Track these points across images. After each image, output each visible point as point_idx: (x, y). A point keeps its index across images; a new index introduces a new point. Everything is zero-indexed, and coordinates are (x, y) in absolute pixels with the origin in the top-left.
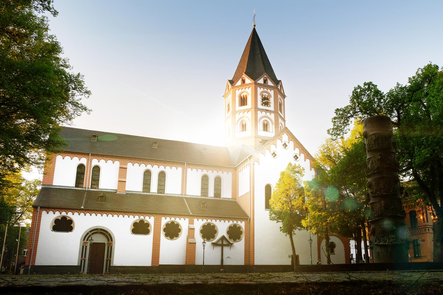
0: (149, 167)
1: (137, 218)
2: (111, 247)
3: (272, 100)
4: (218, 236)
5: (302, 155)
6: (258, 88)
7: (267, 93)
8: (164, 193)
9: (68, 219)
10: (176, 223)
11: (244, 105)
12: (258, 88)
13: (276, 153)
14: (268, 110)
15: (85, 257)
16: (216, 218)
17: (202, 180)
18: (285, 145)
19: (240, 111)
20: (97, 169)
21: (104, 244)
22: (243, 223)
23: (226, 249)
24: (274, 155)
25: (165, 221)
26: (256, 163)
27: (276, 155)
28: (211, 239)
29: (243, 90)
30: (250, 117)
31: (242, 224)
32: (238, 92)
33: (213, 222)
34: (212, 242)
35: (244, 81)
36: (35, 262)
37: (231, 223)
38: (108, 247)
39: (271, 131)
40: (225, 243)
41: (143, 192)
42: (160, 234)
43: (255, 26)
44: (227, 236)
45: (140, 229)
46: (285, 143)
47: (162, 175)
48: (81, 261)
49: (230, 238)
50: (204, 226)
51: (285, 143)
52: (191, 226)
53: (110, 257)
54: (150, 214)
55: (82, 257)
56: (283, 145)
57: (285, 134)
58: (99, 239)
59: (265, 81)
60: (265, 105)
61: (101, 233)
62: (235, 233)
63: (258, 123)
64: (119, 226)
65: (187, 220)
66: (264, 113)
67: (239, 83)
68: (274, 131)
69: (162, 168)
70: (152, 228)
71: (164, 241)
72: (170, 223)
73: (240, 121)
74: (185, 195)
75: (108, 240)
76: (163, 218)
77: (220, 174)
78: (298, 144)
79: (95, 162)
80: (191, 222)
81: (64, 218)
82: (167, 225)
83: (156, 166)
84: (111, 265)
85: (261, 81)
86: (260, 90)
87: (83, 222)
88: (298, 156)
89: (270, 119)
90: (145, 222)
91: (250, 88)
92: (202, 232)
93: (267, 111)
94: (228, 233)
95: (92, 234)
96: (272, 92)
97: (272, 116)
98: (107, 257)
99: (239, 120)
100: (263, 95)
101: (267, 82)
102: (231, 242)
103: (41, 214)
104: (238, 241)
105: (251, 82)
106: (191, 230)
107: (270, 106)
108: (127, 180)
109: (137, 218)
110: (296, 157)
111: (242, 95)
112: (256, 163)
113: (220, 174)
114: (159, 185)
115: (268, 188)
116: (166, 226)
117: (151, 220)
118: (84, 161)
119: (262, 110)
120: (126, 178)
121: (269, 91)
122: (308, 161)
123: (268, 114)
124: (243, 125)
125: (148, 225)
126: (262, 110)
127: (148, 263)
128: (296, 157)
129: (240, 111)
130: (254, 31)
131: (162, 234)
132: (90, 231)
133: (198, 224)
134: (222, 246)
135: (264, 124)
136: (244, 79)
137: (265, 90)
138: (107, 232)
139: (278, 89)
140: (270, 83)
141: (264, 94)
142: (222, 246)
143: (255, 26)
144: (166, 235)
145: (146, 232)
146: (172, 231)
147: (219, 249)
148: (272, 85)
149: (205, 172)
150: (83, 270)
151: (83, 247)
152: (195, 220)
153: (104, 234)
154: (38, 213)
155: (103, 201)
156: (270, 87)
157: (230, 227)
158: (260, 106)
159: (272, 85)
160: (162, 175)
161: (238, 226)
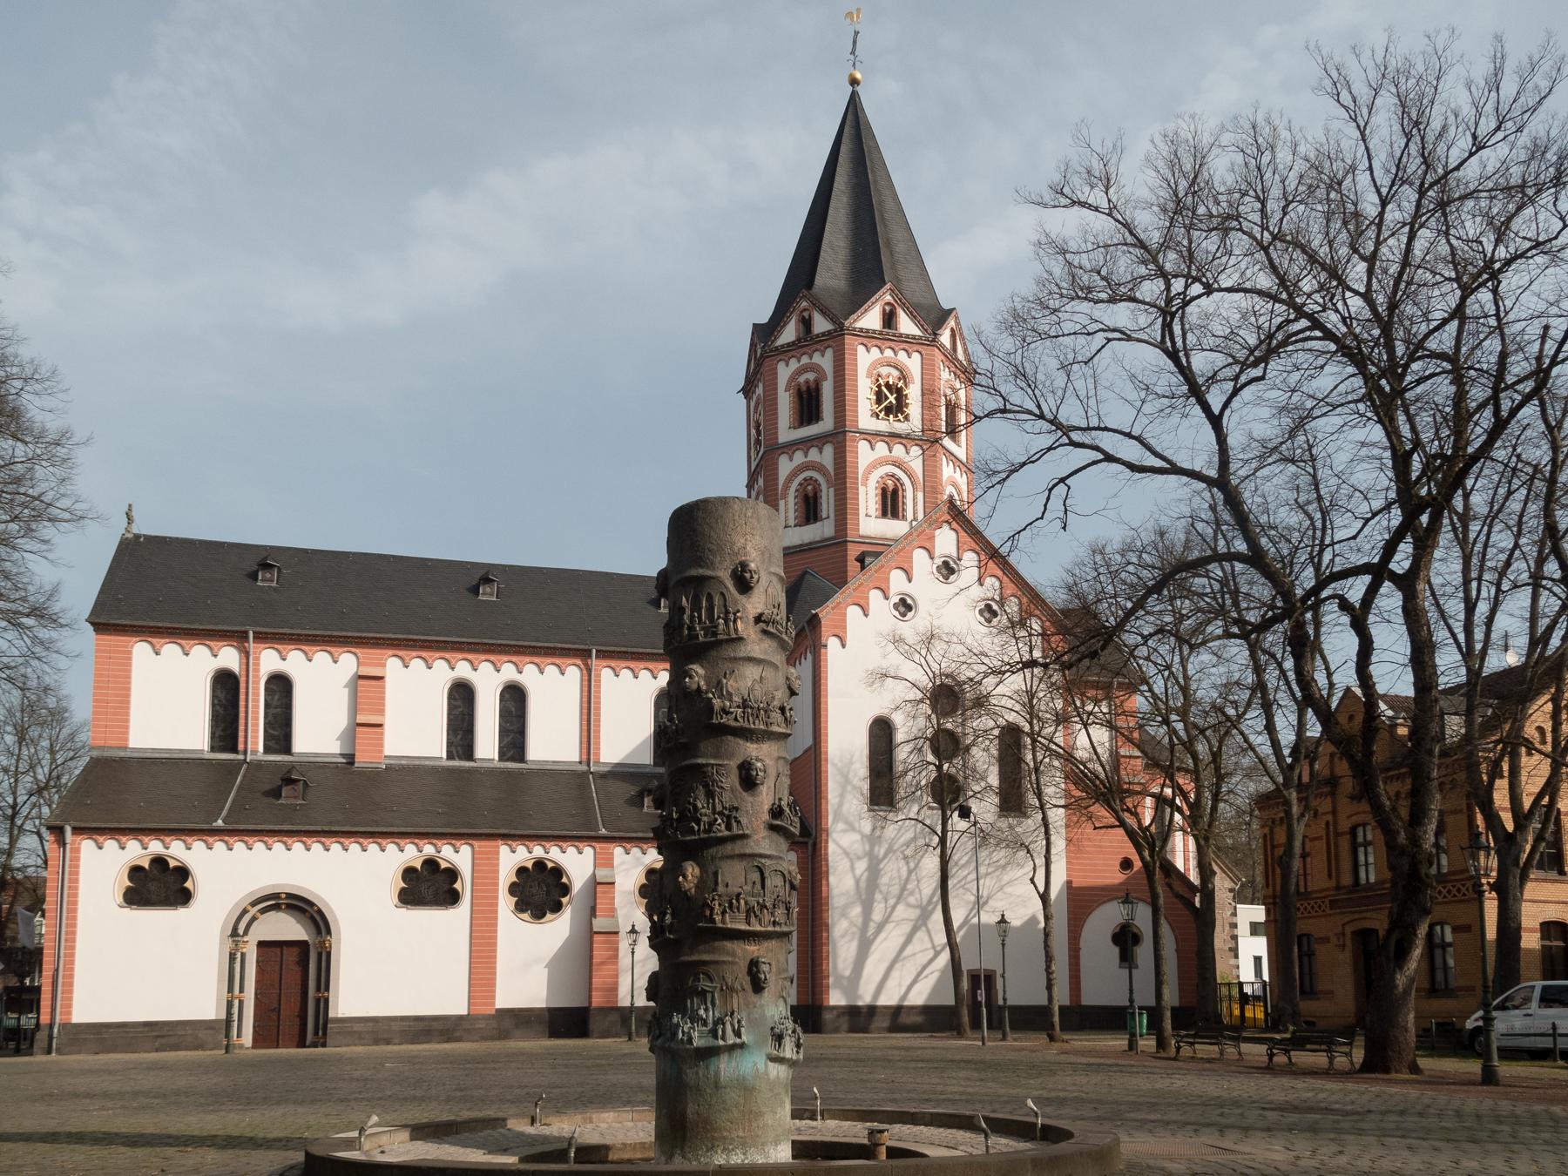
0: (463, 670)
1: (412, 854)
2: (329, 954)
3: (913, 393)
10: (550, 865)
14: (898, 436)
15: (241, 990)
19: (791, 447)
21: (305, 942)
27: (909, 608)
29: (805, 360)
32: (784, 372)
36: (69, 1013)
38: (320, 955)
42: (496, 905)
45: (428, 887)
48: (230, 1005)
52: (602, 874)
53: (327, 989)
55: (230, 989)
58: (288, 928)
59: (889, 319)
60: (887, 415)
61: (289, 907)
64: (353, 880)
65: (588, 851)
66: (881, 448)
67: (789, 334)
69: (509, 672)
70: (465, 885)
71: (510, 924)
72: (529, 865)
75: (319, 932)
76: (504, 850)
79: (269, 660)
80: (604, 861)
82: (522, 871)
84: (331, 1014)
87: (228, 872)
90: (444, 865)
91: (829, 353)
92: (644, 891)
96: (913, 364)
98: (318, 990)
99: (789, 480)
109: (412, 854)
111: (802, 379)
117: (459, 856)
118: (229, 657)
119: (872, 437)
120: (382, 712)
123: (899, 450)
125: (453, 874)
126: (872, 437)
127: (455, 1003)
129: (791, 447)
131: (506, 903)
132: (253, 904)
138: (311, 904)
139: (941, 347)
141: (885, 371)
144: (520, 907)
145: (453, 898)
148: (916, 331)
152: (618, 851)
153: (303, 911)
159: (916, 331)
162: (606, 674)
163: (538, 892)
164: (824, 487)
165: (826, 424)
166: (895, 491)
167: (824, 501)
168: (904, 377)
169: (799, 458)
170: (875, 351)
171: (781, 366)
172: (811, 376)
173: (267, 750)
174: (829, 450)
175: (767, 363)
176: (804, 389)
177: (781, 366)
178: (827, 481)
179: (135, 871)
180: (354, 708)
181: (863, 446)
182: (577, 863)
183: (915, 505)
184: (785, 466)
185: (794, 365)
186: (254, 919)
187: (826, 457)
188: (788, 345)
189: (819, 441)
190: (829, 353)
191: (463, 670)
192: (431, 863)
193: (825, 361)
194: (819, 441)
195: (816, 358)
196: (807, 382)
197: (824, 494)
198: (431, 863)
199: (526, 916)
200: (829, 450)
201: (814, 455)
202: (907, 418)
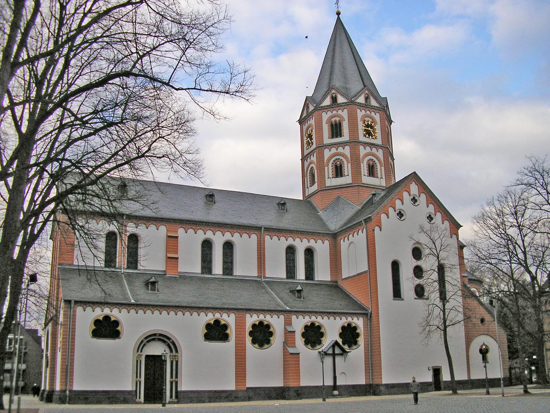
0: (209, 235)
2: (177, 362)
3: (378, 128)
4: (327, 342)
5: (439, 215)
6: (358, 110)
8: (231, 274)
9: (113, 319)
11: (337, 137)
13: (402, 212)
15: (140, 378)
16: (322, 313)
17: (287, 254)
18: (414, 200)
20: (134, 239)
22: (361, 319)
23: (338, 359)
24: (400, 215)
25: (251, 320)
26: (377, 229)
28: (318, 347)
29: (335, 112)
30: (348, 155)
31: (359, 322)
32: (325, 116)
33: (319, 320)
34: (320, 350)
35: (334, 99)
37: (343, 321)
39: (379, 176)
40: (337, 351)
41: (202, 273)
43: (338, 14)
44: (340, 341)
45: (216, 332)
46: (414, 198)
47: (228, 246)
49: (344, 344)
50: (306, 327)
51: (414, 198)
54: (229, 310)
56: (412, 199)
57: (414, 183)
58: (156, 349)
61: (159, 340)
62: (349, 335)
65: (282, 317)
66: (368, 149)
68: (384, 177)
69: (228, 236)
70: (232, 331)
71: (251, 349)
73: (331, 161)
74: (265, 277)
76: (248, 316)
77: (312, 243)
78: (432, 198)
79: (131, 228)
81: (107, 318)
82: (254, 326)
83: (219, 234)
84: (179, 389)
86: (360, 114)
88: (432, 216)
89: (377, 158)
91: (346, 110)
93: (372, 145)
94: (341, 335)
95: (148, 342)
96: (377, 117)
97: (380, 153)
98: (172, 377)
100: (365, 121)
101: (370, 101)
102: (347, 350)
103: (75, 311)
104: (355, 347)
105: (346, 101)
106: (289, 334)
107: (376, 138)
108: (180, 255)
110: (430, 218)
111: (333, 120)
112: (377, 229)
113: (312, 243)
114: (224, 262)
115: (395, 266)
116: (252, 327)
117: (229, 319)
119: (365, 144)
120: (177, 252)
121: (373, 114)
122: (446, 223)
123: (374, 150)
124: (336, 167)
126: (365, 144)
128: (430, 218)
131: (249, 340)
132: (146, 338)
133: (299, 324)
134: (334, 355)
135: (369, 165)
136: (334, 95)
137: (368, 112)
138: (169, 339)
140: (373, 103)
141: (367, 119)
142: (334, 355)
143: (338, 14)
144: (254, 342)
145: (225, 337)
146: (262, 335)
147: (328, 360)
149: (290, 241)
150: (140, 398)
151: (137, 361)
152: (294, 317)
153: (164, 342)
154: (72, 310)
155: (155, 290)
156: (373, 108)
157: (343, 328)
160: (228, 246)
161: (354, 325)
162: (267, 238)
163: (261, 337)
164: (345, 162)
165: (346, 137)
168: (374, 121)
169: (334, 150)
170: (363, 111)
171: (324, 114)
172: (337, 119)
173: (128, 268)
174: (347, 148)
176: (334, 123)
177: (324, 114)
179: (97, 322)
180: (167, 251)
181: (361, 148)
182: (277, 323)
184: (327, 153)
185: (329, 114)
186: (144, 345)
187: (347, 151)
188: (327, 106)
189: (343, 144)
191: (209, 235)
192: (217, 322)
193: (344, 114)
194: (343, 144)
195: (340, 112)
196: (335, 121)
197: (346, 165)
198: (217, 322)
199: (257, 345)
200: (347, 148)
201: (340, 150)
202: (376, 138)
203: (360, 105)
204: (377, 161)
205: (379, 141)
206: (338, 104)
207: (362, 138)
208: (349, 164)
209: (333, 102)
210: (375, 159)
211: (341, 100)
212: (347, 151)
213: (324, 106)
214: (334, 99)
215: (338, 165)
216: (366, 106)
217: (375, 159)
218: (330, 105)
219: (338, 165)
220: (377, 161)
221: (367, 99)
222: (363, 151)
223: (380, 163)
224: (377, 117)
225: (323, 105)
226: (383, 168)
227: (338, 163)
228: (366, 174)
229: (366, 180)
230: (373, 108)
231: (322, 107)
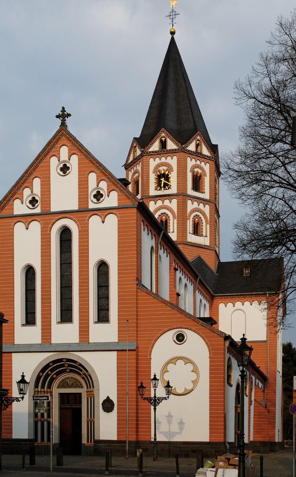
6: (189, 159)
7: (201, 168)
12: (189, 159)
29: (163, 160)
30: (175, 210)
32: (153, 163)
35: (163, 144)
39: (204, 235)
63: (188, 221)
67: (155, 146)
85: (192, 147)
86: (191, 163)
91: (175, 158)
97: (207, 209)
101: (201, 149)
121: (203, 164)
129: (156, 198)
130: (173, 44)
136: (163, 139)
137: (198, 162)
140: (205, 151)
158: (190, 192)
166: (198, 223)
167: (171, 224)
169: (159, 203)
170: (193, 160)
171: (151, 160)
174: (175, 201)
175: (144, 158)
178: (173, 216)
181: (189, 202)
183: (206, 229)
185: (158, 161)
187: (174, 204)
188: (156, 152)
190: (175, 158)
193: (173, 161)
200: (175, 201)
201: (167, 202)
203: (190, 153)
204: (203, 218)
205: (206, 195)
206: (167, 151)
207: (190, 192)
208: (176, 221)
209: (162, 148)
210: (201, 216)
211: (171, 145)
212: (174, 204)
213: (153, 152)
214: (163, 144)
215: (164, 221)
216: (197, 154)
217: (201, 216)
218: (158, 151)
219: (164, 221)
220: (203, 218)
221: (197, 146)
222: (191, 206)
223: (206, 221)
224: (207, 167)
225: (151, 150)
226: (208, 226)
227: (164, 217)
228: (191, 232)
229: (192, 238)
230: (204, 157)
231: (150, 152)
